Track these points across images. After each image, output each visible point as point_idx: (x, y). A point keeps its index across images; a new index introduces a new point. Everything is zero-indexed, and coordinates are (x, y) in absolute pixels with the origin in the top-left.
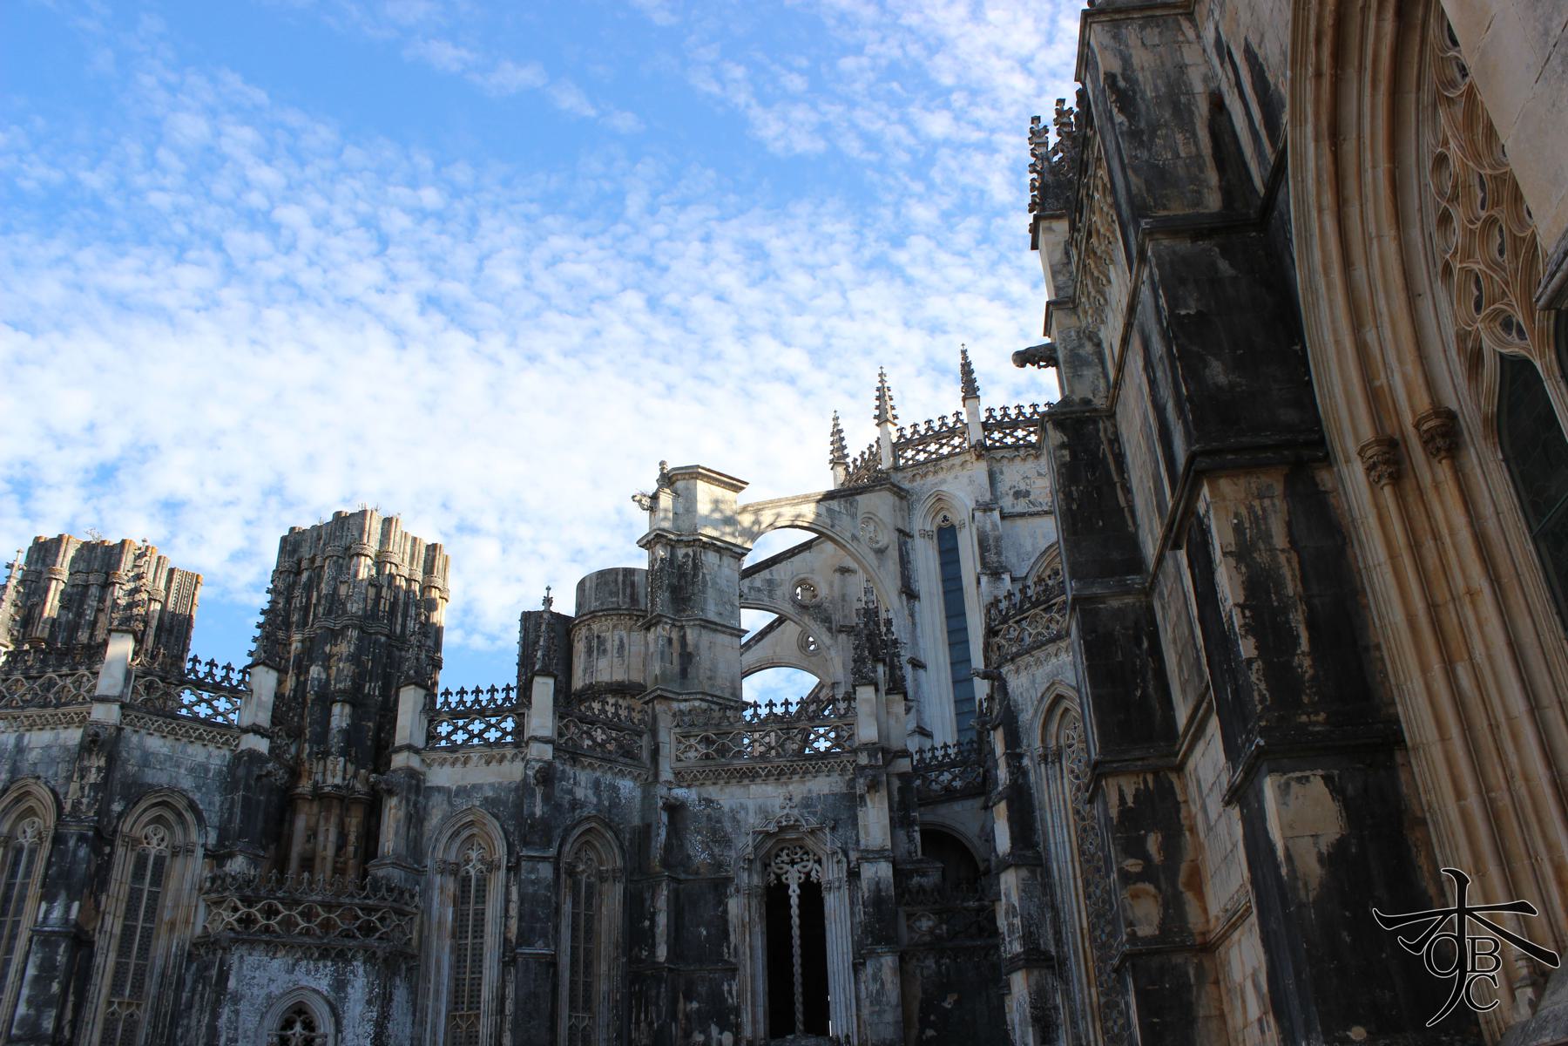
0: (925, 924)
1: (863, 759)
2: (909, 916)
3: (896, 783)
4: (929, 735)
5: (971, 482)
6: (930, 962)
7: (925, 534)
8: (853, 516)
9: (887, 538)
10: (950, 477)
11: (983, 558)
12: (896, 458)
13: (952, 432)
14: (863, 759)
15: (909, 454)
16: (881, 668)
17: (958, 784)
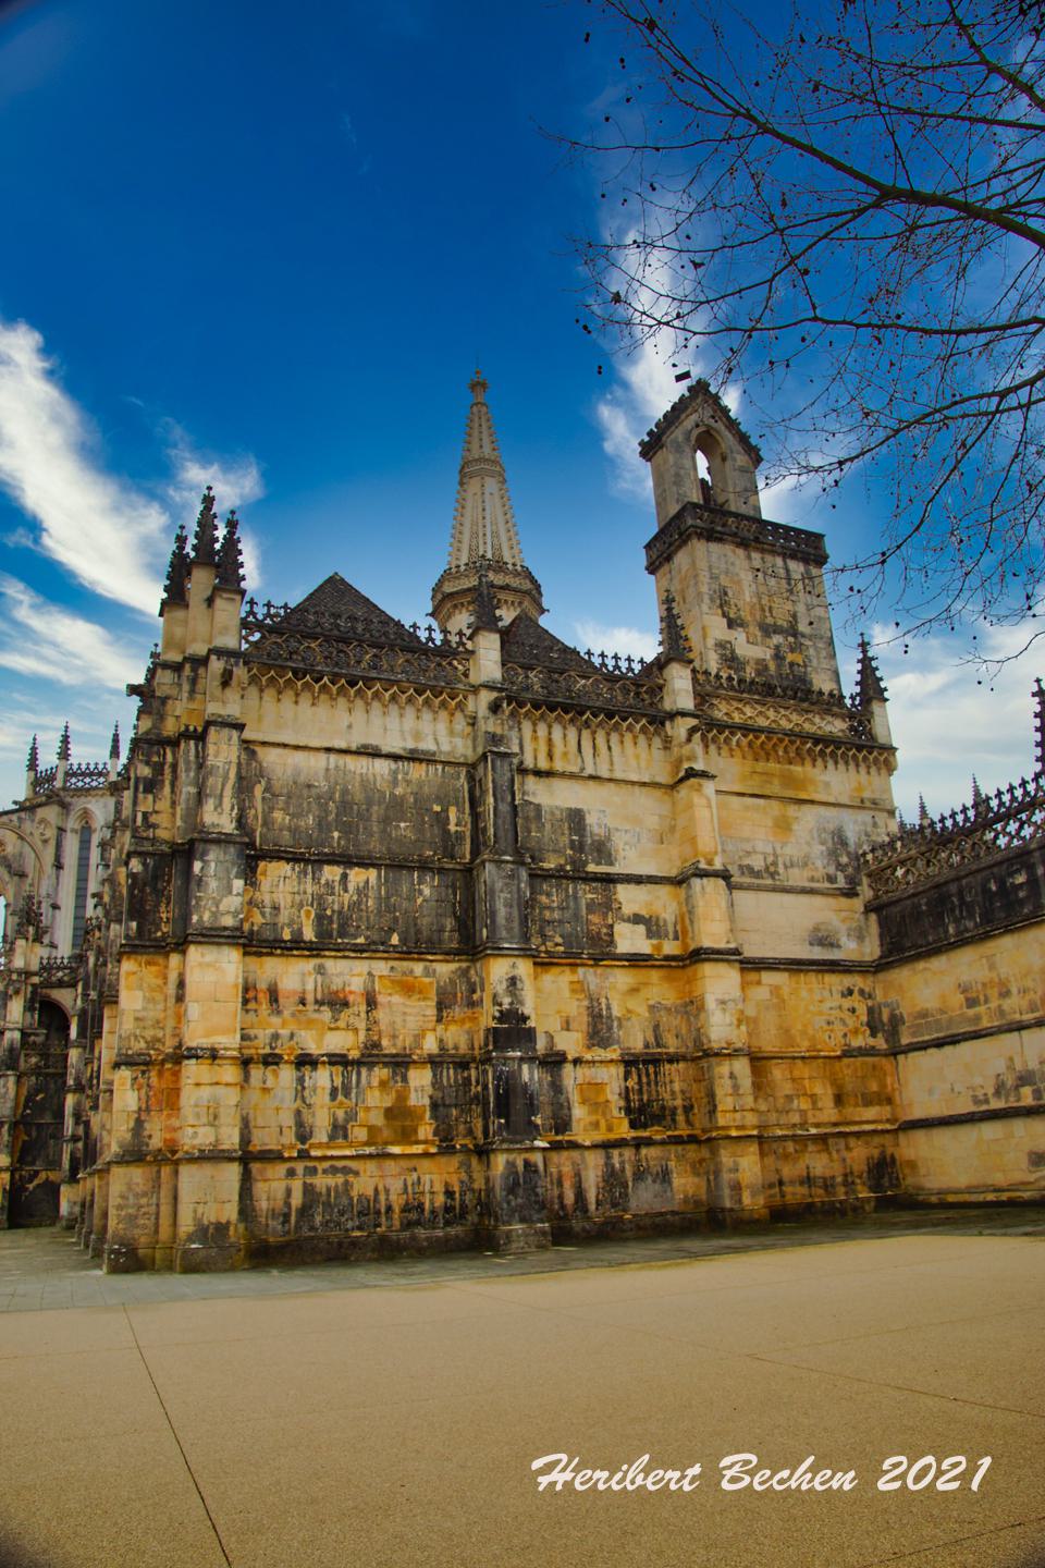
0: (34, 1060)
1: (15, 977)
2: (26, 1055)
3: (30, 989)
4: (56, 947)
5: (105, 806)
6: (33, 1078)
7: (73, 831)
8: (33, 821)
9: (51, 833)
10: (94, 800)
11: (102, 855)
12: (65, 781)
13: (100, 774)
14: (15, 977)
15: (74, 780)
16: (31, 929)
17: (66, 978)
